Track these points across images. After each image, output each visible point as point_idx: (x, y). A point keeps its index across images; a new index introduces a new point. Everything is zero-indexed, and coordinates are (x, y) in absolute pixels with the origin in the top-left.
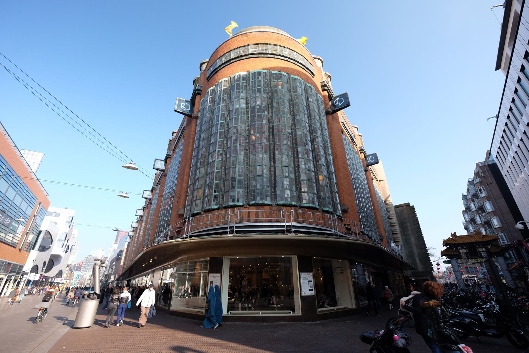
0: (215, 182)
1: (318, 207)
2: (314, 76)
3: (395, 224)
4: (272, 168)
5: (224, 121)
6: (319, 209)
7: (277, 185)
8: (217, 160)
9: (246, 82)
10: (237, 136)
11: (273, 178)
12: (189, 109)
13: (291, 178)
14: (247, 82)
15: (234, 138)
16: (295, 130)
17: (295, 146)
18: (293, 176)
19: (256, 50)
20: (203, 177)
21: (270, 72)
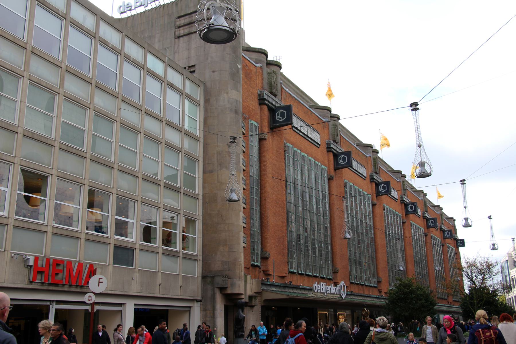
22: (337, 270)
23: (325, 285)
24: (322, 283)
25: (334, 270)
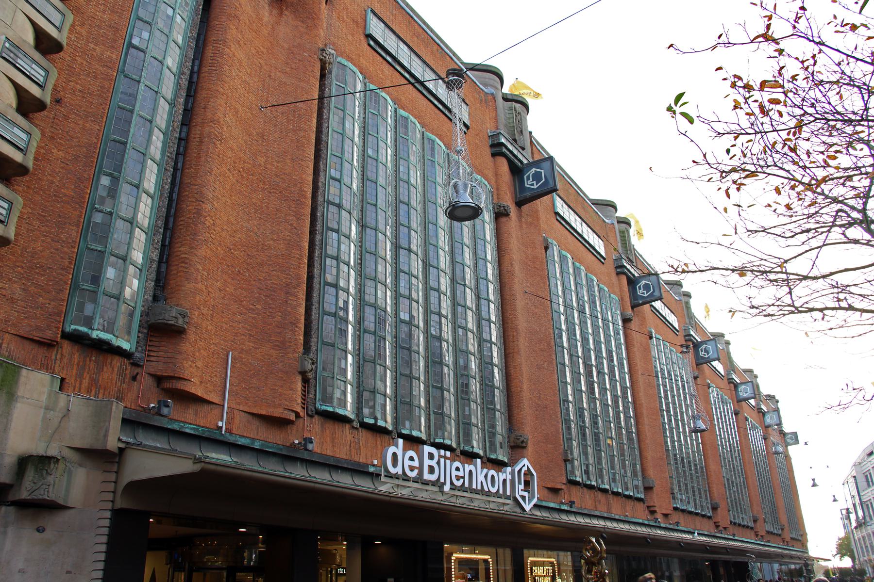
22: (522, 439)
23: (445, 458)
25: (512, 439)
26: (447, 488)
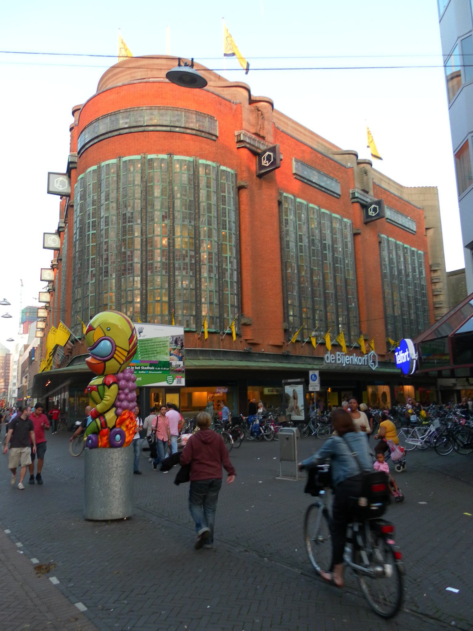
0: (90, 308)
1: (194, 330)
2: (217, 137)
3: (442, 304)
4: (144, 291)
5: (95, 232)
6: (196, 331)
7: (148, 311)
8: (91, 282)
9: (116, 175)
10: (107, 255)
11: (144, 303)
12: (66, 187)
13: (163, 302)
14: (117, 176)
15: (104, 257)
16: (174, 239)
17: (172, 261)
18: (166, 299)
19: (128, 121)
20: (80, 299)
21: (144, 158)
24: (338, 353)
26: (344, 365)
